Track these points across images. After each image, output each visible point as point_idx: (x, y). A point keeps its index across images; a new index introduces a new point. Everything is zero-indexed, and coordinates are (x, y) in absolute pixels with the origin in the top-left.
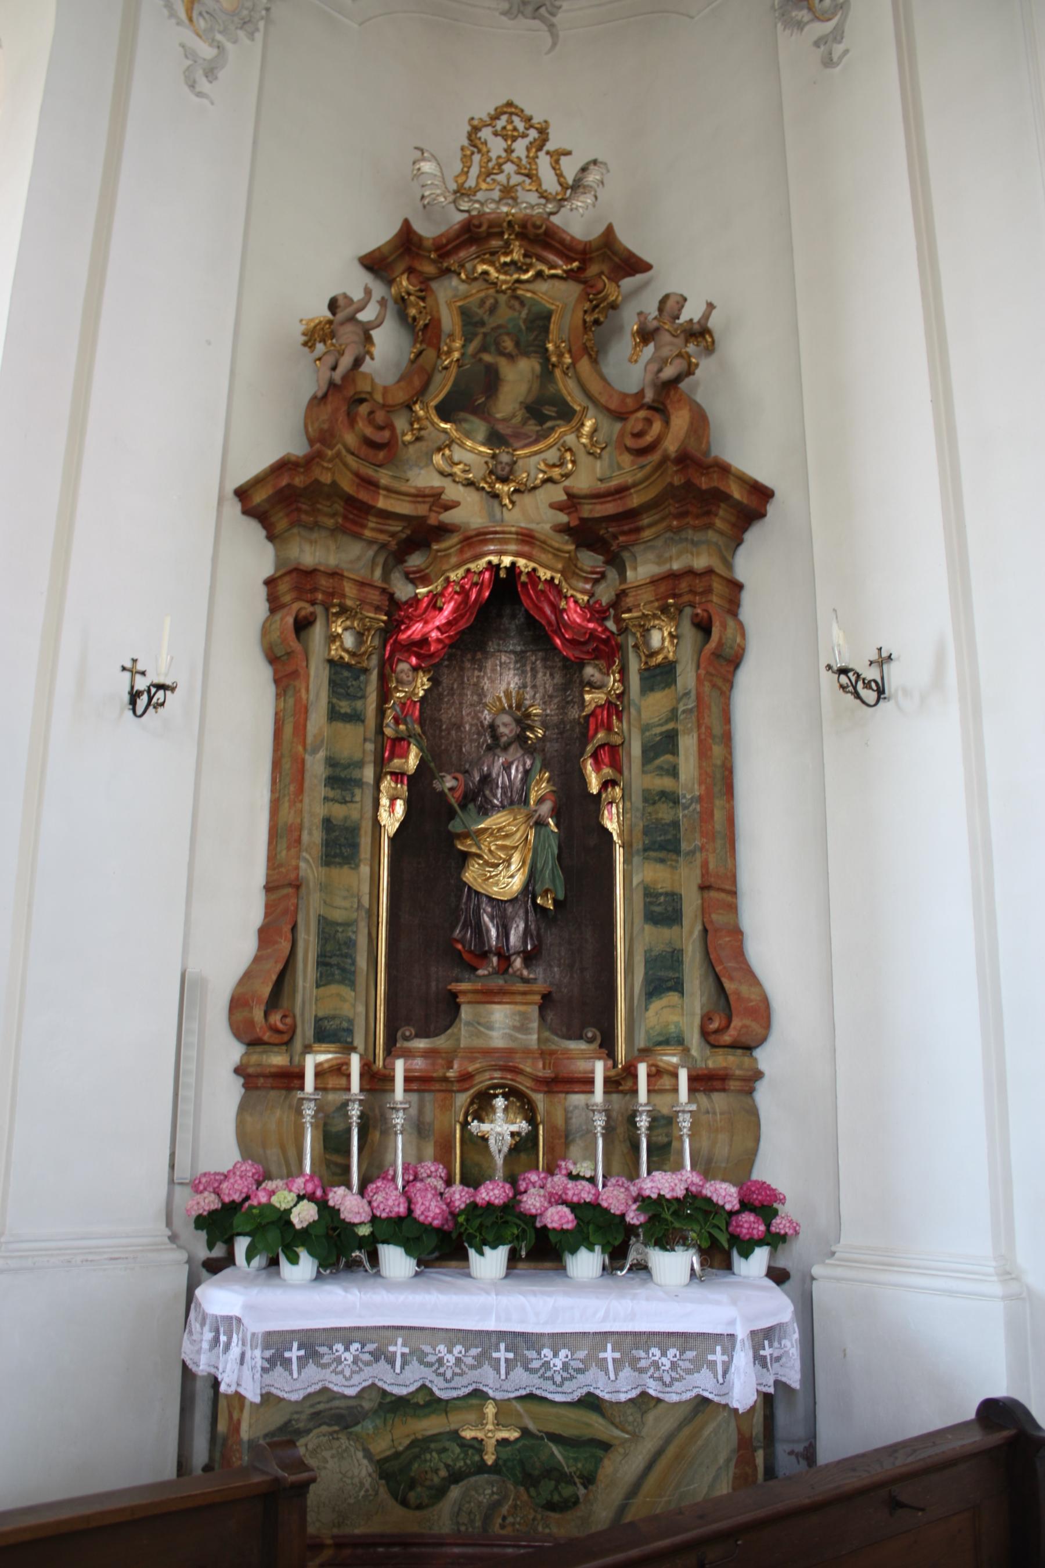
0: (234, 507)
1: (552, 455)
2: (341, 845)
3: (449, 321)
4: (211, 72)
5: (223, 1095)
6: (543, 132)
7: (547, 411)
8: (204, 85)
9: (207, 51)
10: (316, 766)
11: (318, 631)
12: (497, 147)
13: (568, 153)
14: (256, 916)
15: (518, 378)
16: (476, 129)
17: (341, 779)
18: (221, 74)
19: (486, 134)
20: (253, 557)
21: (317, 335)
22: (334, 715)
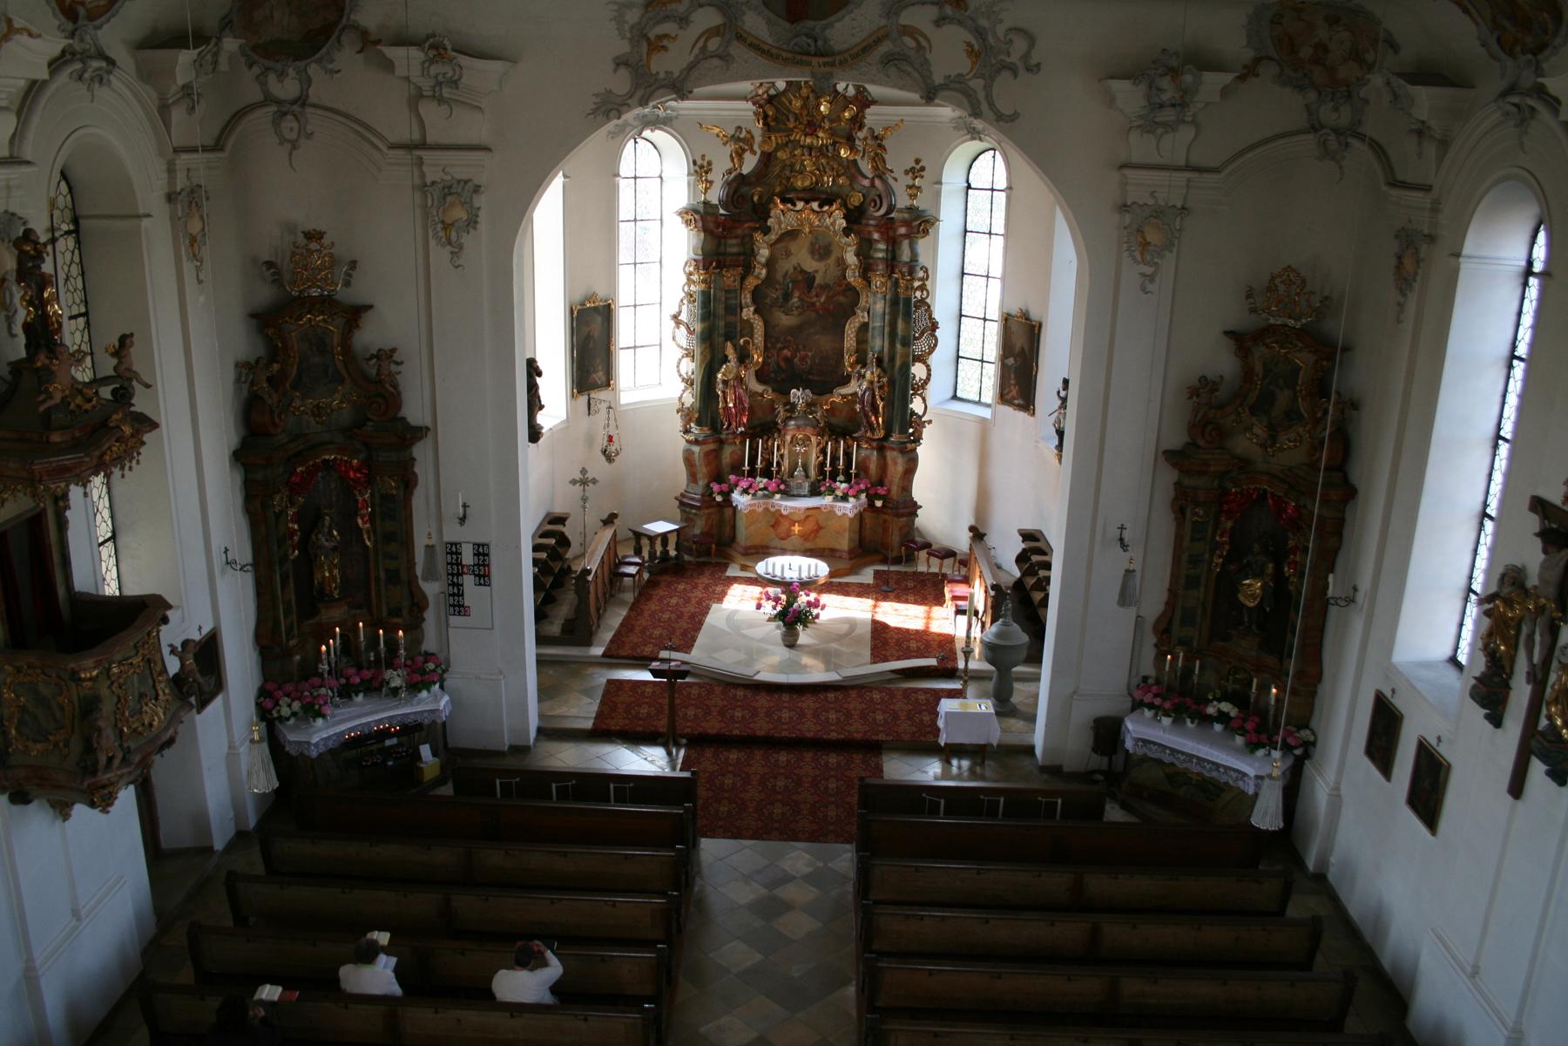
0: (1161, 460)
1: (1292, 436)
2: (1192, 583)
3: (1258, 368)
4: (1152, 280)
5: (1149, 653)
6: (1304, 281)
7: (1292, 416)
8: (1150, 287)
9: (1149, 270)
10: (1185, 557)
11: (1188, 514)
12: (1282, 288)
13: (1312, 293)
14: (1164, 596)
15: (1283, 398)
16: (1273, 278)
17: (1194, 561)
18: (1157, 279)
19: (1277, 281)
20: (1169, 476)
21: (1194, 392)
22: (1192, 540)
